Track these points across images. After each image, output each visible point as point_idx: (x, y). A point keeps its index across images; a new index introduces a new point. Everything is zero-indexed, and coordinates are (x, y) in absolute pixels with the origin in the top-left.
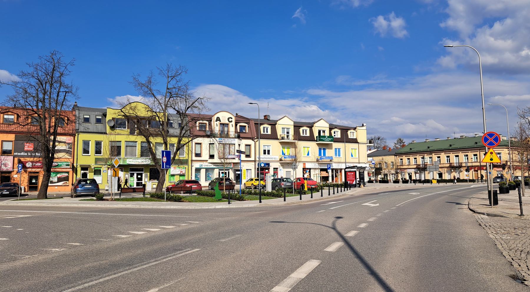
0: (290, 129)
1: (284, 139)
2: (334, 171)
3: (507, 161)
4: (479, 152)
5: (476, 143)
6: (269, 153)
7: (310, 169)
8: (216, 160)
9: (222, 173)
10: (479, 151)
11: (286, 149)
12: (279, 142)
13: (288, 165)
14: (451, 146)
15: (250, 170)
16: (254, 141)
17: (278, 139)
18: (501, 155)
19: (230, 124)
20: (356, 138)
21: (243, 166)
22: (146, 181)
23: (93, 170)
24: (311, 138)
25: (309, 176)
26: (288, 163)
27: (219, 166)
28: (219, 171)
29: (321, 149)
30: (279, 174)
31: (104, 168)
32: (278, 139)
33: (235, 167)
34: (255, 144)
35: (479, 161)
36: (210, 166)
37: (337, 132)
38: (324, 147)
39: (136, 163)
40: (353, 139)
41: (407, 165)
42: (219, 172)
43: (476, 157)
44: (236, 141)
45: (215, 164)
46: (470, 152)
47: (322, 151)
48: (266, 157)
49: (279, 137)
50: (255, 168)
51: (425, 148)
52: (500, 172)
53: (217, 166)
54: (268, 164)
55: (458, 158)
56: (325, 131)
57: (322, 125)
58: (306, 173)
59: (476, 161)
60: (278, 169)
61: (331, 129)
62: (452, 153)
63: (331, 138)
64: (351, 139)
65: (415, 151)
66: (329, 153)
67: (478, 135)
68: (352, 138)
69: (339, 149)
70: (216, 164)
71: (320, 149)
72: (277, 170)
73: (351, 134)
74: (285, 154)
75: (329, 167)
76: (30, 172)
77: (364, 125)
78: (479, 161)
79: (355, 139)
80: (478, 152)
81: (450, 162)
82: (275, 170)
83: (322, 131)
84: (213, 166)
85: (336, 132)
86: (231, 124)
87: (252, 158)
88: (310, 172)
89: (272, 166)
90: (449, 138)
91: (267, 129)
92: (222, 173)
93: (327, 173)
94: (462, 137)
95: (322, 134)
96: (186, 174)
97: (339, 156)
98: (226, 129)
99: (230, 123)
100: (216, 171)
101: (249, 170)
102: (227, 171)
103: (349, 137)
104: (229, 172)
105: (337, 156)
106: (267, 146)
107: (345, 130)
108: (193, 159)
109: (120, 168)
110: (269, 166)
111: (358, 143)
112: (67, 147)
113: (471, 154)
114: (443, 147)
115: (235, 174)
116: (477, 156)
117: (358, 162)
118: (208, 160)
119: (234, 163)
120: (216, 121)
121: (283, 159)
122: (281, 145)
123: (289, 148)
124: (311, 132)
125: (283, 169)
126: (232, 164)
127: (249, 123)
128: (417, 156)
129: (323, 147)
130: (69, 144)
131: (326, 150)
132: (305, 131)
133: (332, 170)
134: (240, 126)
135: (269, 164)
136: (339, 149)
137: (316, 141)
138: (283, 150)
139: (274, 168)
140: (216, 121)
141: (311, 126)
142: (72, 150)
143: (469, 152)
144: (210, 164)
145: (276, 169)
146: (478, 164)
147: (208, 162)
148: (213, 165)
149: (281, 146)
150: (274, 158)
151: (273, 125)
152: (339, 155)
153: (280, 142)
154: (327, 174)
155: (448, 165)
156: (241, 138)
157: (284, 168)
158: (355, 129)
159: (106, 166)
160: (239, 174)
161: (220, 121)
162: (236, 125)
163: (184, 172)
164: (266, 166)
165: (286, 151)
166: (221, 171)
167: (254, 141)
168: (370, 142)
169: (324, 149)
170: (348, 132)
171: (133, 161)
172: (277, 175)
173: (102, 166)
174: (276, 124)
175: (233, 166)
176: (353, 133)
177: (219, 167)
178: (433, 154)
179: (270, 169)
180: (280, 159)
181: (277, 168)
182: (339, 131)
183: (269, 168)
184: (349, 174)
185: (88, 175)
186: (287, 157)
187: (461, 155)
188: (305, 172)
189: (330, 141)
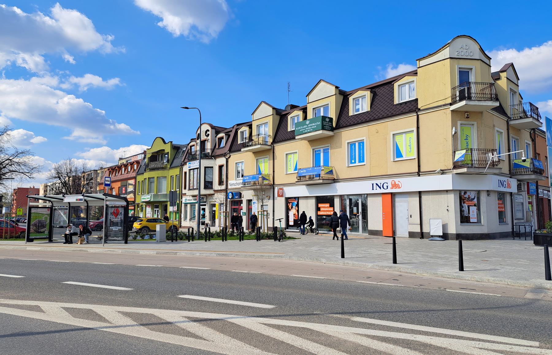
25: (297, 214)
33: (210, 201)
54: (240, 195)
58: (292, 207)
63: (315, 123)
69: (361, 143)
88: (298, 205)
93: (330, 206)
97: (360, 162)
105: (355, 162)
117: (417, 171)
136: (361, 143)
145: (249, 201)
152: (361, 160)
154: (332, 209)
188: (290, 206)
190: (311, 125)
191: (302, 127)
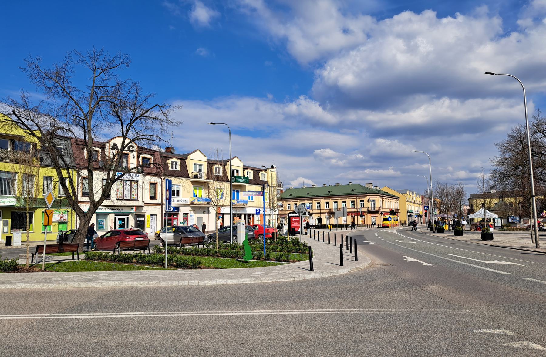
0: (202, 166)
1: (198, 177)
2: (247, 216)
3: (379, 208)
4: (356, 199)
5: (353, 190)
6: (178, 195)
7: (223, 214)
9: (119, 219)
10: (356, 198)
11: (198, 190)
13: (200, 209)
14: (329, 192)
15: (154, 215)
16: (161, 179)
17: (190, 178)
19: (131, 154)
20: (266, 180)
21: (147, 210)
22: (4, 231)
24: (223, 179)
25: (222, 222)
26: (200, 208)
27: (115, 210)
28: (115, 217)
29: (235, 191)
30: (190, 221)
32: (190, 178)
34: (162, 182)
35: (356, 207)
36: (104, 209)
37: (250, 172)
38: (238, 190)
40: (264, 181)
41: (350, 209)
42: (115, 218)
44: (139, 178)
45: (109, 208)
46: (348, 198)
47: (236, 193)
48: (175, 199)
49: (190, 175)
50: (162, 214)
51: (305, 194)
52: (374, 218)
53: (113, 209)
54: (178, 209)
55: (337, 204)
56: (239, 171)
57: (236, 164)
58: (219, 219)
60: (188, 215)
61: (244, 169)
62: (331, 199)
63: (246, 179)
64: (262, 181)
65: (323, 196)
66: (242, 196)
67: (351, 183)
68: (263, 180)
70: (112, 208)
71: (234, 191)
72: (187, 217)
73: (263, 176)
74: (196, 197)
75: (257, 212)
77: (274, 167)
78: (356, 207)
79: (266, 181)
80: (355, 198)
81: (330, 208)
82: (185, 215)
83: (235, 171)
84: (107, 210)
85: (248, 173)
86: (131, 154)
87: (158, 201)
88: (223, 218)
89: (183, 210)
90: (326, 185)
91: (176, 164)
92: (119, 219)
93: (239, 218)
94: (337, 185)
95: (236, 174)
96: (69, 220)
97: (251, 200)
98: (124, 160)
99: (131, 153)
100: (111, 217)
101: (153, 216)
102: (125, 217)
103: (261, 179)
104: (128, 218)
105: (249, 200)
106: (176, 186)
107: (256, 172)
110: (179, 211)
113: (348, 201)
114: (322, 194)
115: (136, 221)
116: (346, 203)
119: (136, 206)
120: (112, 149)
121: (196, 202)
123: (201, 189)
124: (225, 171)
125: (194, 215)
126: (134, 207)
127: (154, 155)
128: (297, 201)
129: (237, 189)
131: (239, 193)
132: (218, 170)
133: (245, 215)
134: (143, 158)
135: (179, 208)
138: (195, 191)
139: (184, 214)
140: (112, 149)
141: (224, 164)
143: (347, 199)
145: (186, 214)
146: (355, 210)
148: (107, 209)
149: (193, 187)
150: (184, 201)
151: (183, 159)
153: (192, 182)
155: (328, 211)
156: (144, 173)
157: (195, 213)
158: (266, 170)
160: (141, 221)
162: (138, 157)
163: (65, 218)
164: (176, 211)
165: (198, 192)
166: (117, 217)
167: (161, 179)
169: (238, 192)
170: (259, 174)
172: (187, 222)
174: (187, 159)
175: (136, 210)
176: (264, 174)
177: (115, 211)
178: (313, 200)
179: (179, 215)
180: (191, 202)
181: (187, 214)
182: (252, 172)
183: (178, 214)
184: (293, 219)
186: (201, 200)
187: (340, 201)
189: (246, 183)
190: (244, 180)
191: (239, 179)
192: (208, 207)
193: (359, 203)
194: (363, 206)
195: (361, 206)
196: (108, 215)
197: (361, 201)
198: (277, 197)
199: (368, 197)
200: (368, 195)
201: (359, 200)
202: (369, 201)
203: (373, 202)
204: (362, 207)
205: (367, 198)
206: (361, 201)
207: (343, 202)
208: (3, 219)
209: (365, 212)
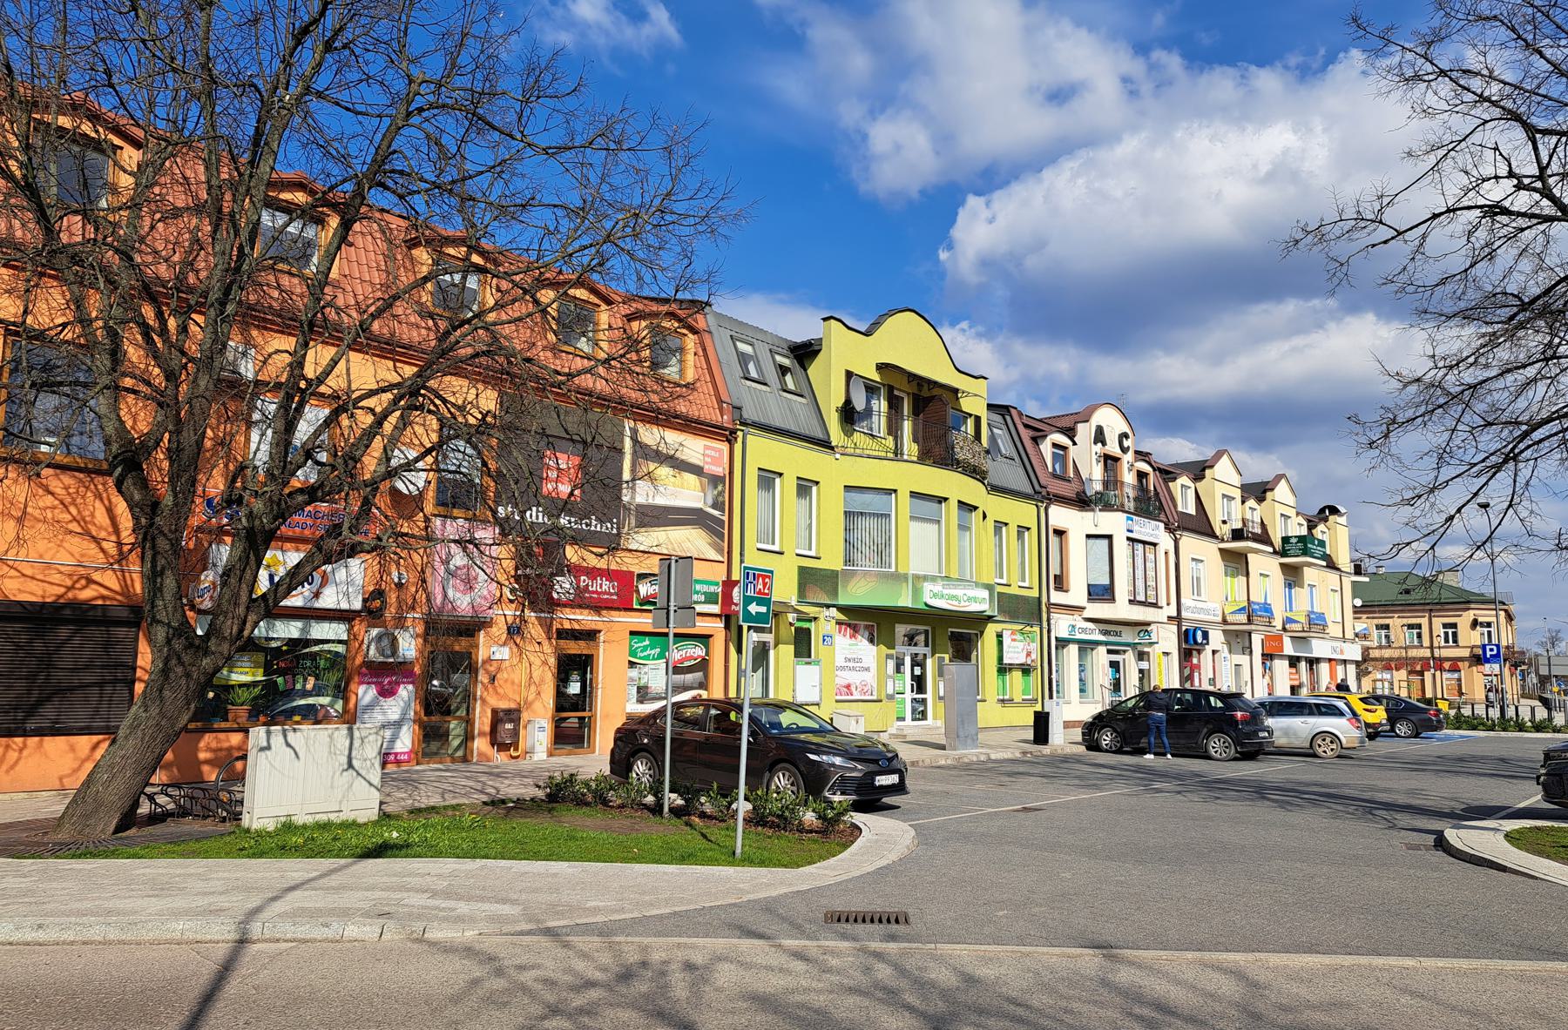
4: (1426, 619)
8: (1121, 609)
12: (1220, 549)
18: (1492, 629)
23: (793, 628)
31: (825, 624)
35: (1426, 643)
36: (1092, 631)
39: (956, 603)
43: (1415, 631)
49: (1219, 529)
53: (1106, 633)
59: (1416, 643)
76: (563, 634)
78: (1426, 643)
108: (1052, 601)
109: (867, 627)
111: (1338, 569)
112: (710, 502)
118: (1084, 608)
122: (1223, 560)
123: (1233, 576)
130: (715, 480)
137: (1284, 553)
140: (1095, 443)
142: (725, 518)
143: (1392, 617)
144: (1091, 625)
147: (1087, 614)
159: (833, 611)
161: (1104, 444)
168: (1358, 570)
171: (945, 592)
173: (817, 609)
185: (772, 653)
192: (1250, 634)
193: (1439, 630)
194: (1455, 641)
195: (1447, 641)
196: (1092, 649)
197: (1445, 626)
198: (1355, 607)
199: (1472, 612)
200: (1473, 606)
201: (1438, 623)
202: (1475, 624)
203: (1486, 630)
204: (1451, 643)
205: (1469, 616)
206: (1445, 626)
207: (1410, 627)
208: (937, 655)
209: (1462, 659)
